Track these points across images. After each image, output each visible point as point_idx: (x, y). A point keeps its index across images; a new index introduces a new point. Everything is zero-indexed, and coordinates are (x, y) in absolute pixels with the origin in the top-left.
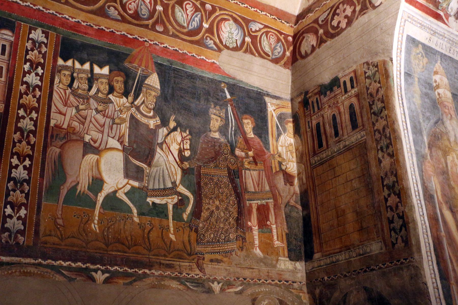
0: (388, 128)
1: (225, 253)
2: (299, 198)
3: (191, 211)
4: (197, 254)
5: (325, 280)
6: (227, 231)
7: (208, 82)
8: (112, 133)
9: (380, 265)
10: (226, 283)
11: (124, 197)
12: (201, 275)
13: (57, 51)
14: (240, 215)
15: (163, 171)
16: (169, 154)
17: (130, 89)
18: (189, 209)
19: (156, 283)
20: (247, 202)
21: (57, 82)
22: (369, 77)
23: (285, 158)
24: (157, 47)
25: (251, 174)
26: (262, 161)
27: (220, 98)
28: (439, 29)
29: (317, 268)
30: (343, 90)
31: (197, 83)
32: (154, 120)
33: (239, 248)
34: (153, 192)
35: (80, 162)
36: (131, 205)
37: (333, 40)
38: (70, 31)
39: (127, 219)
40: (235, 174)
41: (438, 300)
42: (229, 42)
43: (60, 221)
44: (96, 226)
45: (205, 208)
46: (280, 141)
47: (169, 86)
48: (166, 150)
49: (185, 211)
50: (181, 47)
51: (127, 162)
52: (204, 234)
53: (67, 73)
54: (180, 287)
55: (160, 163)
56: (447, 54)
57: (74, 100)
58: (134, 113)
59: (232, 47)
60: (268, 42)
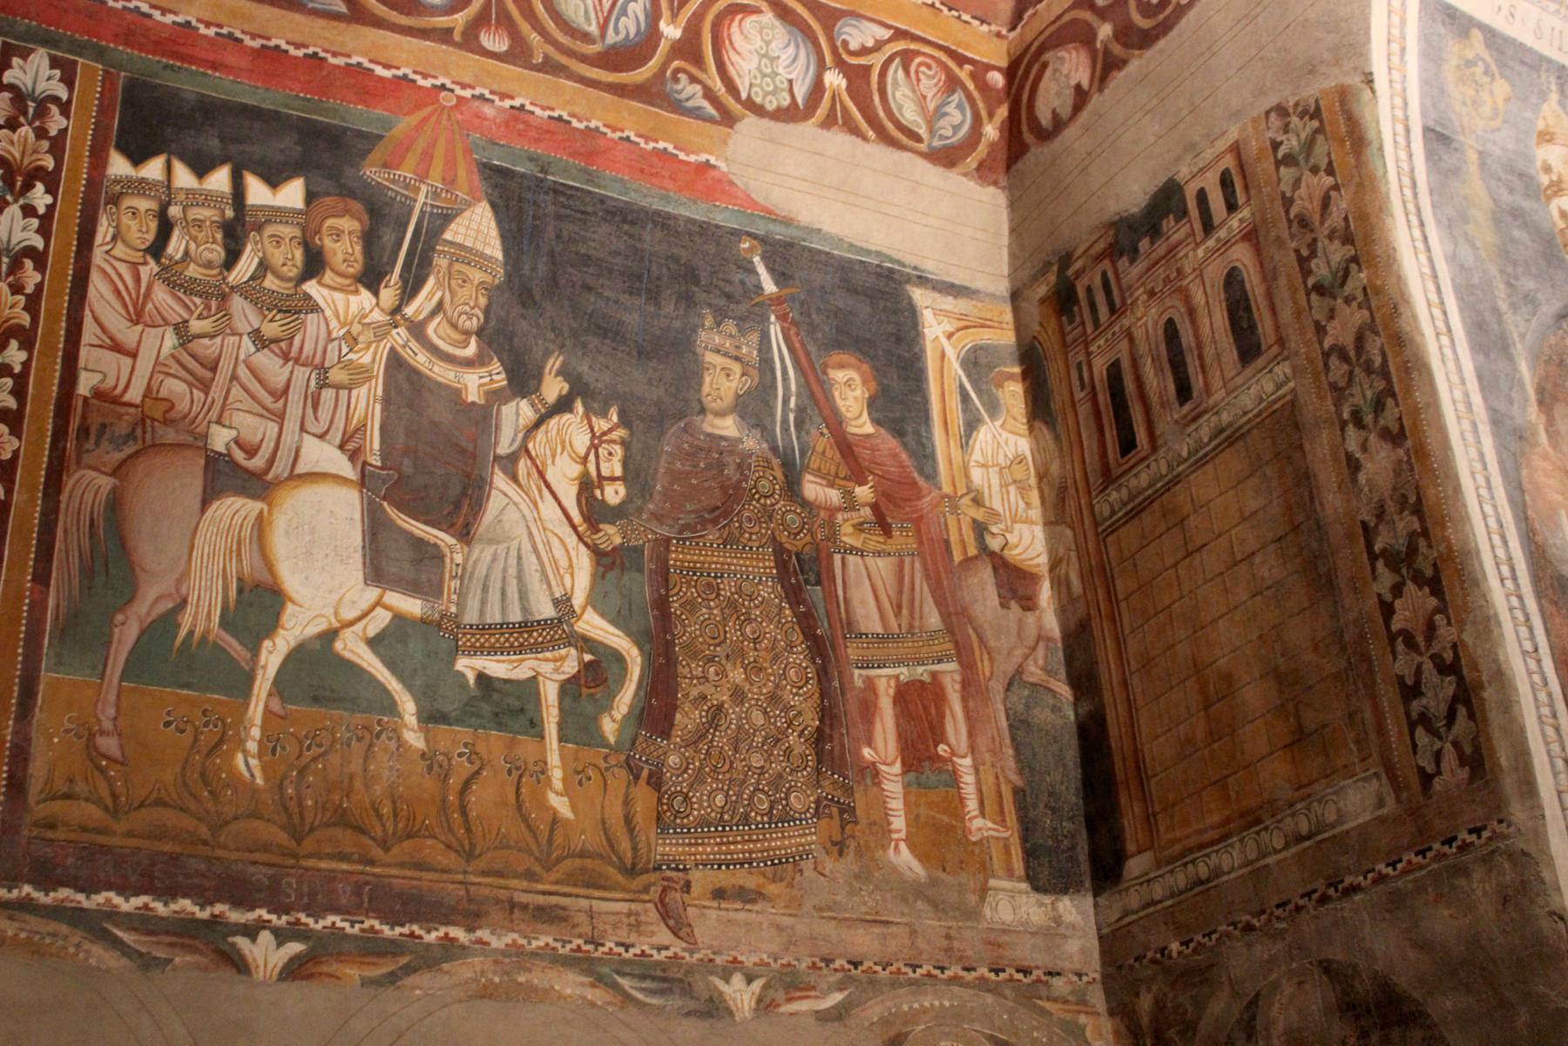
0: (1377, 333)
1: (773, 864)
2: (1061, 654)
3: (631, 706)
4: (660, 866)
5: (1170, 957)
7: (690, 235)
8: (316, 419)
9: (1381, 867)
10: (781, 980)
11: (365, 657)
12: (677, 947)
13: (109, 128)
14: (828, 722)
15: (519, 558)
16: (541, 497)
17: (385, 260)
18: (625, 699)
19: (497, 980)
20: (857, 672)
21: (105, 237)
22: (1289, 160)
23: (1000, 510)
24: (488, 111)
25: (867, 568)
26: (909, 520)
27: (737, 292)
29: (1142, 914)
30: (1197, 225)
31: (647, 236)
32: (483, 371)
33: (829, 845)
34: (482, 635)
35: (193, 526)
36: (393, 685)
37: (1148, 54)
38: (157, 58)
39: (378, 735)
40: (806, 567)
42: (760, 86)
43: (109, 744)
44: (254, 762)
45: (686, 695)
46: (977, 446)
47: (538, 248)
48: (533, 483)
49: (608, 708)
50: (577, 110)
51: (375, 528)
52: (687, 795)
53: (144, 204)
54: (597, 995)
55: (507, 526)
57: (171, 301)
58: (403, 347)
59: (775, 105)
60: (914, 91)
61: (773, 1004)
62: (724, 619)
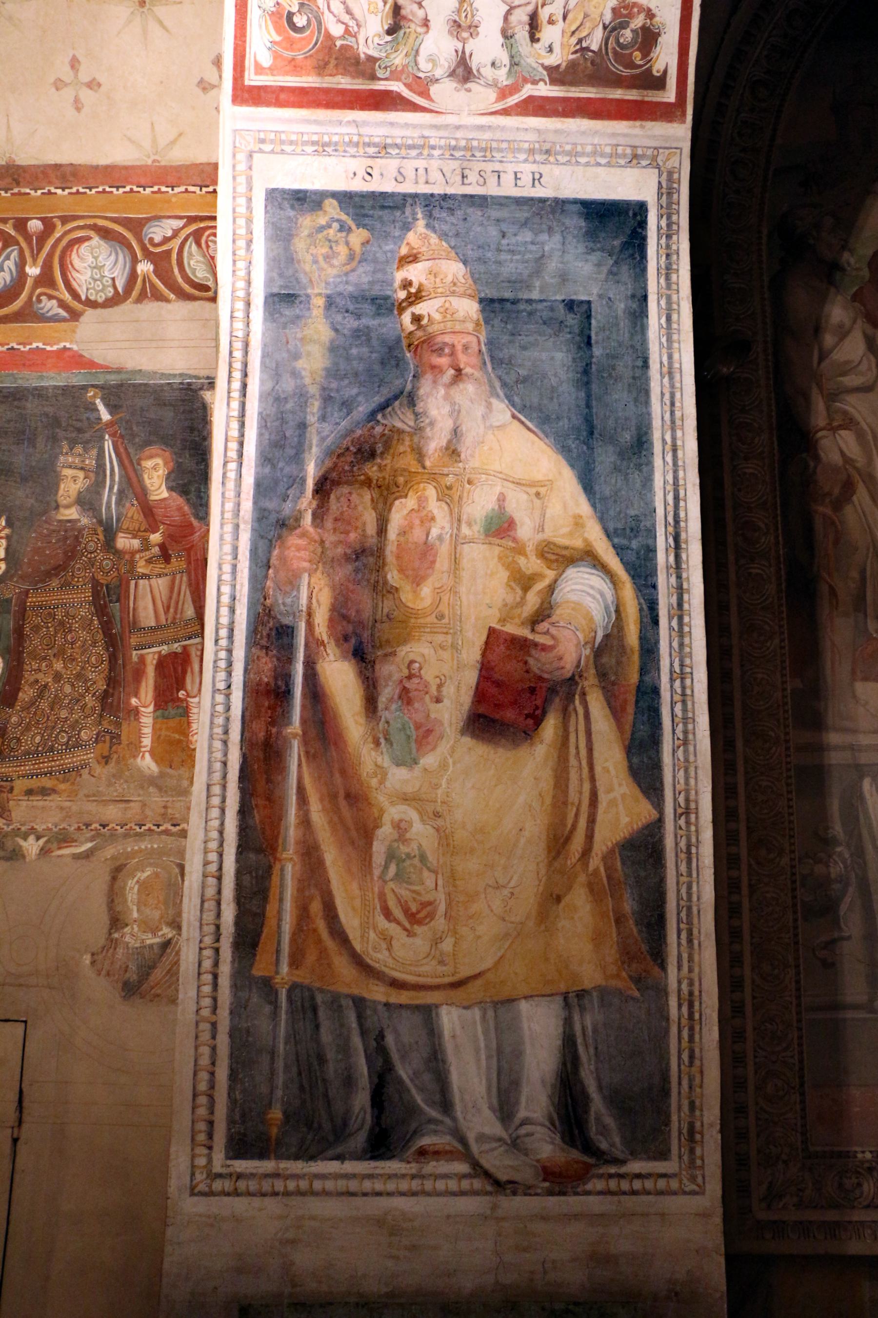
6: (73, 727)
20: (134, 653)
26: (185, 550)
28: (397, 132)
31: (29, 405)
33: (100, 759)
41: (210, 905)
56: (450, 191)
60: (204, 256)
61: (50, 851)
62: (56, 633)
